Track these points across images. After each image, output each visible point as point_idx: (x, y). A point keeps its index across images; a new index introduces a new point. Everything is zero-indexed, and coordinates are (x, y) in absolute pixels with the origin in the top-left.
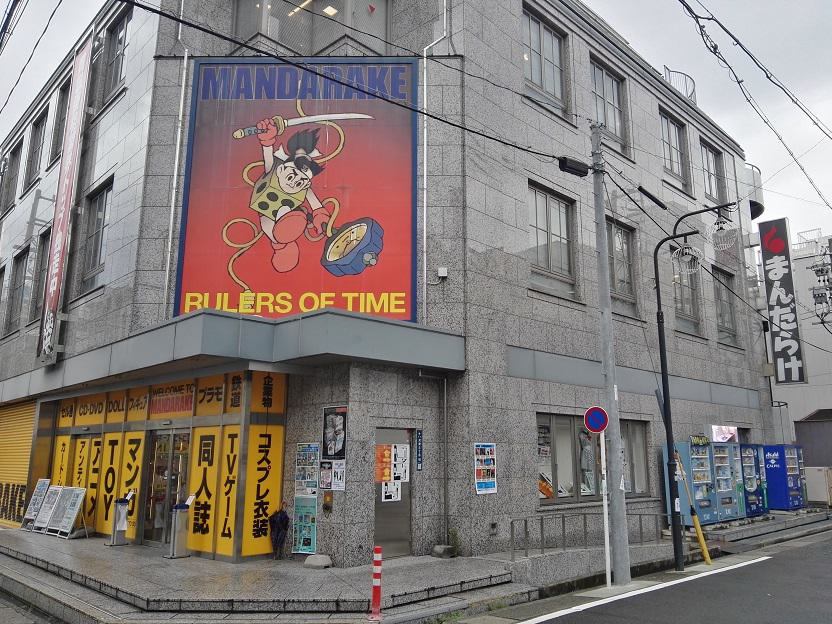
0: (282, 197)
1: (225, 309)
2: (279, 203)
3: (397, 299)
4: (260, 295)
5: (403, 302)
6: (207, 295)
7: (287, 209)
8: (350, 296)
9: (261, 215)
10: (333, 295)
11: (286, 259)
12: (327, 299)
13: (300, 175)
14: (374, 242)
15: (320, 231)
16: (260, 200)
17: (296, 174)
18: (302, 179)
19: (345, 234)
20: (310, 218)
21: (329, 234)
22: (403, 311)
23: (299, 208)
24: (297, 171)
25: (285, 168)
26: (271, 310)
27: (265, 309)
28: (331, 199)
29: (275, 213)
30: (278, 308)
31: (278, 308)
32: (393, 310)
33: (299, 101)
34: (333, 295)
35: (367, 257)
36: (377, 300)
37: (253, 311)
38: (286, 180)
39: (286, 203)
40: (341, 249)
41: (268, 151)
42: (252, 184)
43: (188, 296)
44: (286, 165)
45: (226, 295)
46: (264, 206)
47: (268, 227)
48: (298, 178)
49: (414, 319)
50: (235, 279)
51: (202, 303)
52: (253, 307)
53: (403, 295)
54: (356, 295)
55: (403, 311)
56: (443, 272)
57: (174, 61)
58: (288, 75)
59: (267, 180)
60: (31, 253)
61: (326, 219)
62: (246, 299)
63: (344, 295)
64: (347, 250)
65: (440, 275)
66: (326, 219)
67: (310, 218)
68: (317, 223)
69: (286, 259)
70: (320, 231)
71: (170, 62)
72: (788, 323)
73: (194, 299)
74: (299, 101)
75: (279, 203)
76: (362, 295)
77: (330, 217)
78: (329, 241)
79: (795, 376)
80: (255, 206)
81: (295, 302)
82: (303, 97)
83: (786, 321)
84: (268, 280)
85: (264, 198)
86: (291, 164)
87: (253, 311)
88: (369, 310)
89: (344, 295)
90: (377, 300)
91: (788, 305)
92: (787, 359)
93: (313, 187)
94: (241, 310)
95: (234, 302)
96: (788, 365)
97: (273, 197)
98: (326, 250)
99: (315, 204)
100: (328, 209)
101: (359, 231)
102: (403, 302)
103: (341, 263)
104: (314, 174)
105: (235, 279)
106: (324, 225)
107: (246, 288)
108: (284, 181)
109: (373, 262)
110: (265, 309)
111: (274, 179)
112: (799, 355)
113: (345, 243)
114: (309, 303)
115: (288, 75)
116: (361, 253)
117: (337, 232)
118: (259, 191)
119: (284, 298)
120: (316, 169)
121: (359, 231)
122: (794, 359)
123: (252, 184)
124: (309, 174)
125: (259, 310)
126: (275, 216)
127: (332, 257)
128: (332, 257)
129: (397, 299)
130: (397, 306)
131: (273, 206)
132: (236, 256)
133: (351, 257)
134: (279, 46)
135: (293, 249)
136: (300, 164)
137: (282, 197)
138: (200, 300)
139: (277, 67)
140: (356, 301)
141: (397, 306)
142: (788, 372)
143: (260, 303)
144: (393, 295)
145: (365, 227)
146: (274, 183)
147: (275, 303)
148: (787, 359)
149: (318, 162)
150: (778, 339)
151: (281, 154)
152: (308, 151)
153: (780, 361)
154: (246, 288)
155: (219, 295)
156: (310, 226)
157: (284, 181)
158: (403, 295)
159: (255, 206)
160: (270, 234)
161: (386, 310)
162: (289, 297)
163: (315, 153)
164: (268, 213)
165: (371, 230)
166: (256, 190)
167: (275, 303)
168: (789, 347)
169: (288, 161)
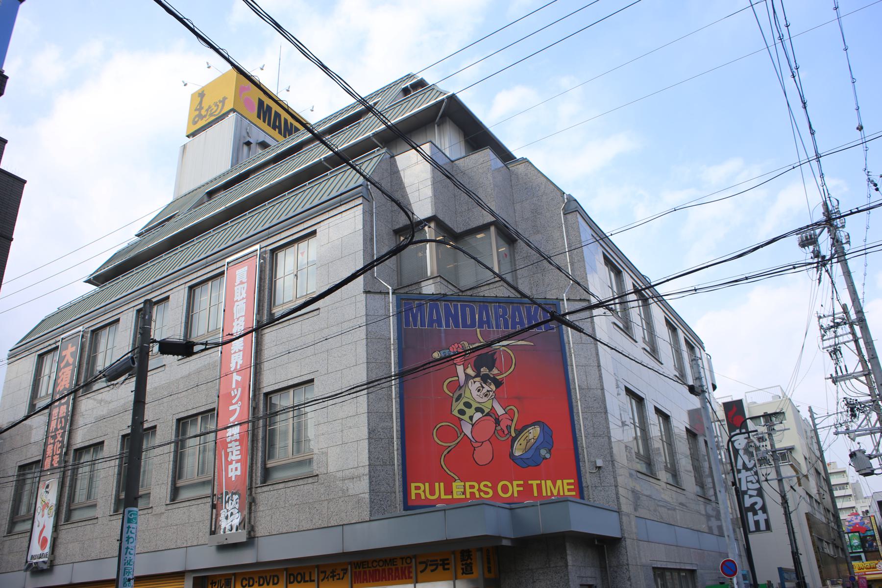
0: (475, 405)
1: (443, 497)
2: (473, 410)
3: (568, 484)
4: (468, 484)
5: (572, 487)
6: (427, 484)
7: (478, 415)
8: (534, 483)
9: (461, 420)
10: (521, 482)
11: (483, 454)
12: (518, 486)
13: (486, 388)
14: (547, 439)
15: (506, 432)
16: (459, 408)
17: (483, 388)
18: (488, 391)
19: (524, 434)
20: (497, 421)
21: (513, 434)
22: (574, 493)
23: (488, 414)
24: (484, 385)
25: (475, 382)
26: (477, 496)
27: (472, 494)
28: (512, 407)
29: (471, 418)
30: (482, 494)
31: (482, 494)
32: (567, 493)
33: (478, 330)
34: (521, 482)
35: (543, 452)
36: (554, 484)
37: (463, 497)
38: (475, 391)
39: (478, 410)
40: (523, 446)
41: (460, 369)
42: (451, 395)
43: (413, 485)
44: (475, 380)
45: (442, 484)
46: (462, 412)
47: (467, 429)
48: (485, 391)
49: (582, 498)
50: (447, 470)
51: (424, 491)
52: (464, 493)
53: (572, 481)
54: (539, 482)
55: (574, 493)
56: (599, 463)
57: (380, 295)
58: (468, 309)
59: (462, 391)
60: (638, 488)
61: (509, 423)
62: (457, 487)
63: (530, 482)
64: (528, 447)
65: (598, 465)
66: (509, 423)
67: (497, 421)
68: (503, 425)
69: (483, 454)
70: (506, 432)
71: (377, 296)
72: (753, 483)
73: (418, 488)
74: (478, 330)
75: (473, 410)
76: (543, 482)
77: (512, 420)
78: (514, 440)
79: (763, 526)
80: (455, 413)
81: (494, 488)
82: (480, 326)
83: (751, 482)
84: (475, 473)
85: (461, 406)
86: (478, 379)
87: (463, 497)
88: (549, 494)
89: (530, 482)
90: (554, 484)
91: (751, 469)
92: (755, 513)
93: (496, 398)
94: (455, 496)
95: (448, 491)
96: (756, 518)
97: (468, 405)
98: (512, 447)
99: (500, 411)
100: (510, 414)
101: (535, 432)
102: (572, 487)
103: (522, 457)
105: (447, 470)
106: (509, 427)
107: (457, 478)
108: (475, 393)
109: (548, 456)
110: (472, 494)
111: (467, 392)
112: (764, 509)
113: (526, 441)
114: (505, 489)
115: (468, 309)
116: (538, 449)
117: (519, 432)
118: (457, 400)
119: (486, 486)
120: (498, 383)
121: (535, 432)
122: (760, 512)
123: (451, 395)
124: (493, 387)
125: (468, 496)
126: (472, 421)
127: (517, 453)
128: (517, 453)
129: (568, 484)
130: (569, 490)
131: (469, 412)
132: (445, 453)
133: (531, 453)
134: (449, 284)
135: (487, 446)
136: (485, 379)
137: (475, 405)
138: (422, 489)
139: (459, 304)
140: (539, 486)
141: (569, 490)
142: (757, 523)
143: (468, 491)
144: (565, 481)
145: (538, 429)
146: (467, 394)
147: (480, 490)
148: (755, 513)
149: (498, 377)
150: (746, 497)
151: (470, 371)
152: (490, 370)
153: (750, 514)
154: (457, 478)
155: (437, 484)
156: (499, 428)
157: (475, 393)
158: (572, 481)
159: (455, 413)
160: (470, 436)
161: (562, 494)
162: (490, 484)
163: (495, 371)
164: (466, 417)
165: (542, 430)
166: (454, 400)
167: (480, 490)
168: (756, 503)
169: (476, 377)
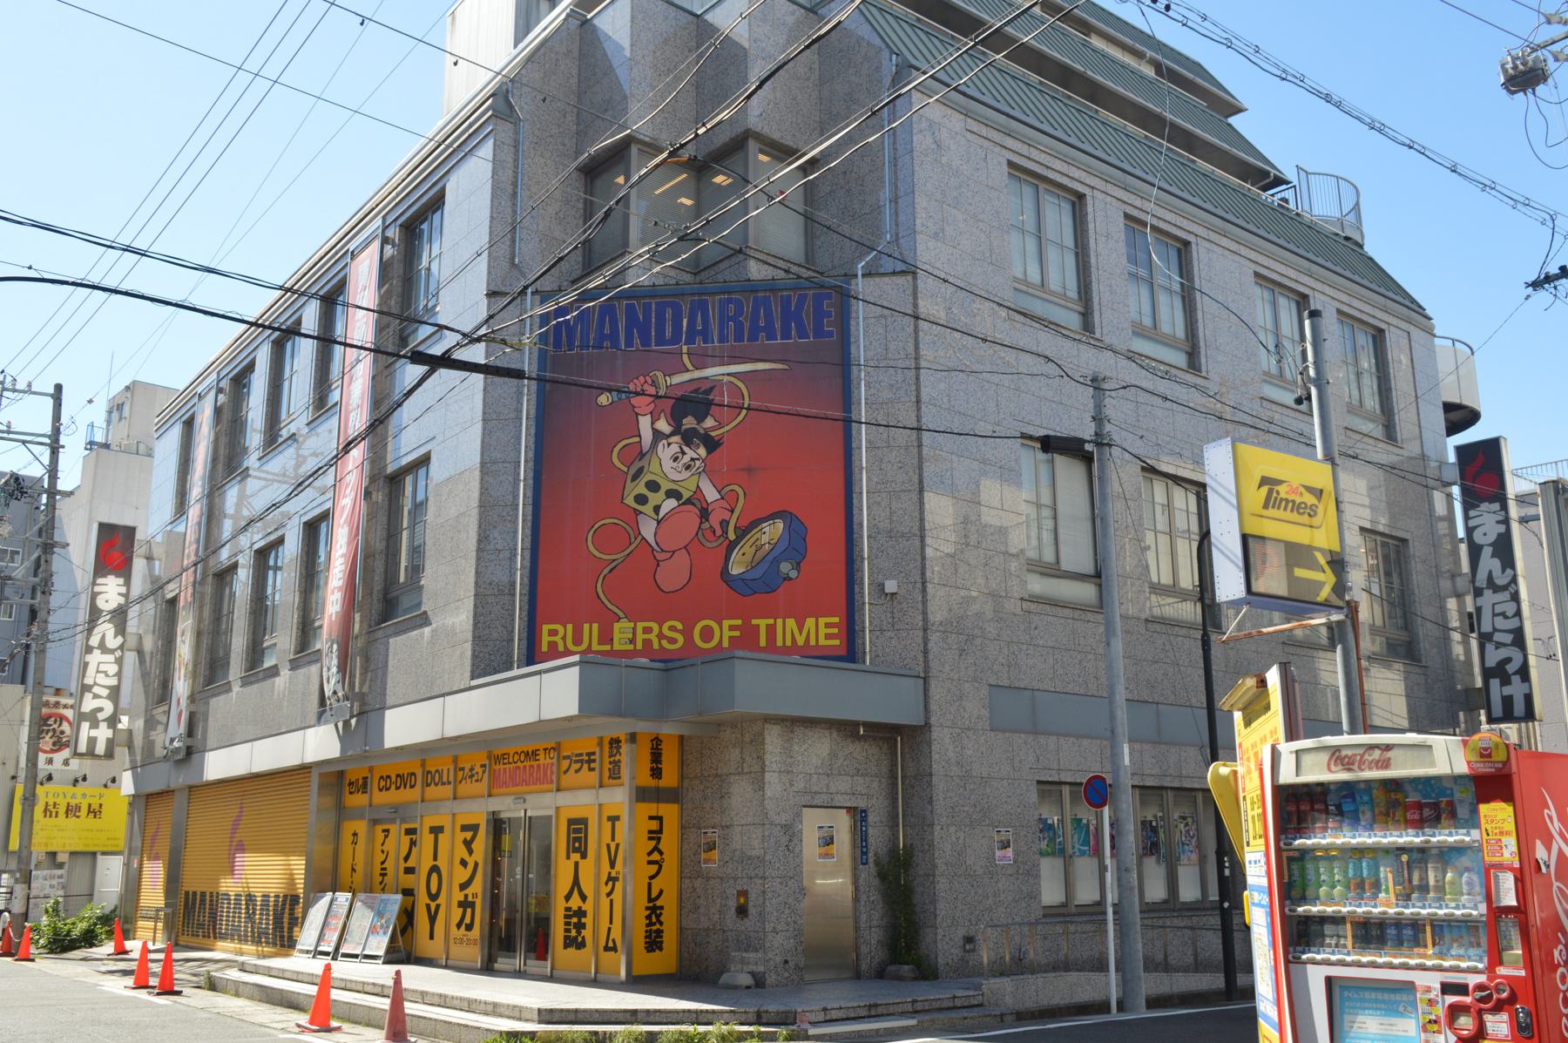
0: (665, 486)
1: (595, 647)
2: (662, 494)
3: (828, 625)
4: (640, 625)
5: (835, 631)
6: (570, 627)
7: (671, 504)
8: (763, 623)
9: (637, 513)
10: (739, 622)
11: (673, 574)
12: (732, 628)
13: (690, 453)
14: (795, 546)
15: (719, 532)
16: (636, 492)
18: (692, 459)
20: (704, 514)
21: (732, 536)
22: (837, 642)
23: (689, 501)
24: (686, 449)
25: (669, 444)
26: (656, 646)
27: (647, 643)
29: (657, 509)
30: (665, 643)
31: (665, 643)
32: (822, 642)
34: (739, 622)
35: (785, 567)
39: (671, 494)
40: (749, 557)
41: (645, 423)
42: (625, 469)
43: (546, 628)
45: (595, 626)
46: (641, 499)
47: (648, 530)
48: (686, 459)
51: (564, 638)
52: (633, 641)
53: (836, 620)
54: (771, 621)
55: (837, 642)
59: (644, 462)
62: (622, 630)
63: (754, 622)
67: (704, 514)
68: (714, 520)
69: (673, 574)
72: (1506, 617)
73: (553, 633)
75: (662, 494)
77: (732, 511)
78: (732, 546)
79: (1519, 708)
80: (630, 501)
81: (688, 633)
82: (690, 341)
83: (1504, 615)
85: (641, 488)
86: (676, 439)
87: (631, 647)
88: (789, 643)
89: (754, 622)
91: (1504, 588)
92: (1506, 681)
93: (708, 471)
94: (617, 647)
96: (1507, 691)
97: (653, 486)
98: (727, 558)
99: (711, 494)
100: (728, 499)
101: (773, 531)
102: (835, 631)
103: (748, 576)
104: (709, 453)
106: (724, 524)
107: (621, 615)
108: (668, 464)
109: (793, 574)
110: (647, 643)
112: (1524, 672)
113: (754, 547)
114: (707, 634)
116: (776, 562)
117: (742, 532)
118: (635, 478)
119: (672, 628)
120: (712, 444)
121: (773, 531)
122: (1516, 679)
123: (625, 469)
124: (702, 451)
125: (639, 646)
127: (736, 570)
128: (736, 570)
129: (828, 625)
130: (828, 636)
131: (654, 498)
132: (606, 571)
135: (682, 559)
136: (689, 438)
137: (665, 486)
138: (561, 633)
139: (653, 301)
140: (771, 630)
141: (828, 636)
142: (1508, 701)
143: (640, 637)
144: (822, 621)
145: (780, 525)
146: (654, 467)
147: (661, 636)
148: (1506, 681)
149: (713, 434)
150: (1489, 647)
151: (663, 426)
152: (700, 420)
153: (1495, 683)
154: (621, 615)
155: (586, 627)
156: (706, 525)
157: (668, 464)
158: (836, 620)
159: (630, 501)
160: (651, 540)
161: (813, 642)
162: (679, 626)
163: (709, 422)
165: (789, 527)
167: (661, 636)
168: (1508, 660)
169: (672, 434)
